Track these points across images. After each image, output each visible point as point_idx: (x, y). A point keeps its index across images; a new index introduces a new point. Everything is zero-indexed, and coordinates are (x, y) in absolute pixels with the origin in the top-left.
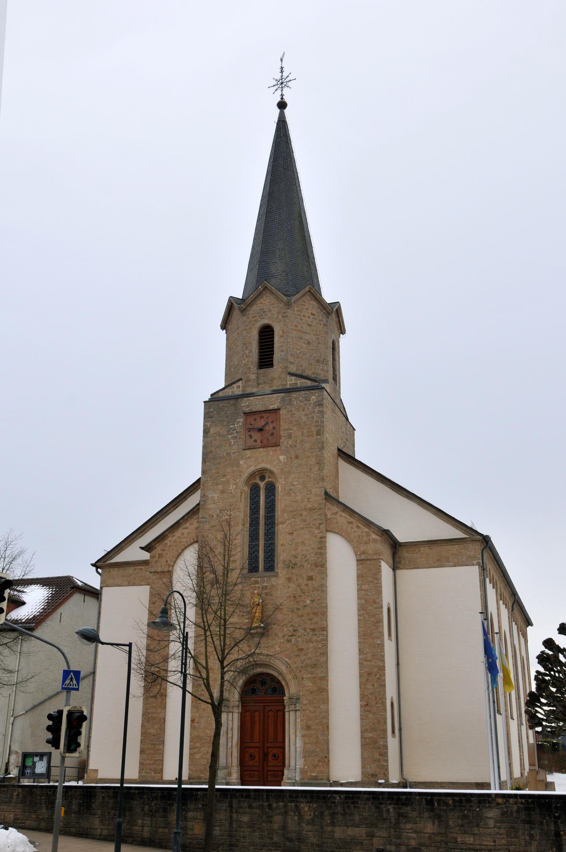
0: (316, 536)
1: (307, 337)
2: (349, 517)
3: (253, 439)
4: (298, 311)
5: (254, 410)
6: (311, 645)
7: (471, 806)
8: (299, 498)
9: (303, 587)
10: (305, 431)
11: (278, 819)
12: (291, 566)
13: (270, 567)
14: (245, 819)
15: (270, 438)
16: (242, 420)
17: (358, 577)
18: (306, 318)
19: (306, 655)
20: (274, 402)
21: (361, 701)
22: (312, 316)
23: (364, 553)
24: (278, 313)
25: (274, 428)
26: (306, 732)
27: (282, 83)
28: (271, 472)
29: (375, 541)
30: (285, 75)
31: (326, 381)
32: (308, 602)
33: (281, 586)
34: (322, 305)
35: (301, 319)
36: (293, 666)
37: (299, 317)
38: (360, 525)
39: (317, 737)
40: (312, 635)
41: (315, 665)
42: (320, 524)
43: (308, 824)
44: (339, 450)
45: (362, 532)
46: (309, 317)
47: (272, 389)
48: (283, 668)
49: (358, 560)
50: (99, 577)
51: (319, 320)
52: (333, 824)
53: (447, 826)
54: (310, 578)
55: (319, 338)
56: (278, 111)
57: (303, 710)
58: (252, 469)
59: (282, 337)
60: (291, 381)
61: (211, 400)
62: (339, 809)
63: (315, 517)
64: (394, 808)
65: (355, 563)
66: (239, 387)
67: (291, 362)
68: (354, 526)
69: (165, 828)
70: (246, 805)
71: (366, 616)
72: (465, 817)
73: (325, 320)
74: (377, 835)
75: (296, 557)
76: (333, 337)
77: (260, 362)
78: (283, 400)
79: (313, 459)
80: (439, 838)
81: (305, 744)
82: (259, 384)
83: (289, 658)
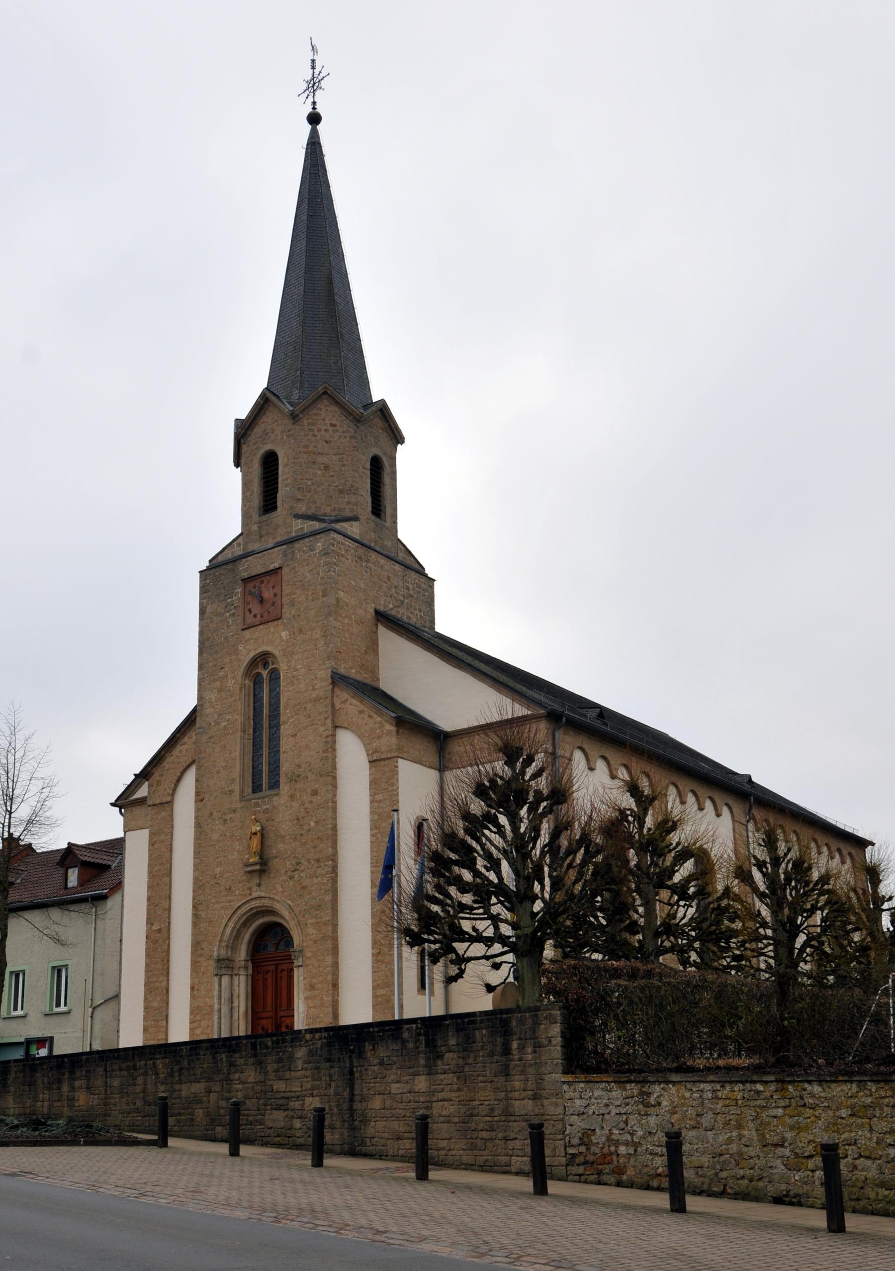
0: (321, 736)
1: (324, 459)
2: (360, 704)
3: (253, 613)
4: (309, 424)
5: (253, 574)
6: (315, 881)
7: (285, 1047)
8: (302, 686)
9: (307, 805)
10: (310, 593)
11: (140, 1080)
12: (295, 779)
13: (275, 785)
14: (116, 1083)
16: (240, 590)
17: (371, 782)
18: (323, 432)
19: (310, 894)
20: (274, 560)
21: (373, 948)
22: (331, 429)
23: (376, 751)
24: (283, 432)
25: (275, 595)
27: (314, 85)
28: (274, 656)
29: (389, 733)
30: (317, 71)
31: (355, 519)
32: (313, 824)
33: (283, 806)
34: (346, 409)
35: (314, 436)
37: (311, 433)
38: (372, 714)
39: (322, 998)
41: (320, 906)
42: (326, 719)
43: (162, 1083)
44: (377, 612)
45: (375, 723)
46: (326, 430)
47: (275, 541)
48: (285, 913)
49: (370, 762)
50: (122, 818)
51: (344, 432)
52: (180, 1082)
53: (266, 1072)
54: (315, 793)
55: (342, 458)
56: (308, 127)
58: (252, 654)
59: (286, 465)
60: (299, 526)
61: (208, 569)
62: (185, 1063)
63: (321, 710)
64: (227, 1056)
65: (367, 765)
66: (239, 545)
67: (299, 500)
68: (366, 716)
69: (59, 1101)
71: (379, 836)
72: (280, 1060)
73: (352, 430)
74: (213, 1089)
75: (299, 766)
76: (375, 451)
77: (265, 506)
78: (285, 554)
79: (319, 631)
80: (258, 1088)
81: (309, 1008)
82: (261, 537)
83: (291, 900)
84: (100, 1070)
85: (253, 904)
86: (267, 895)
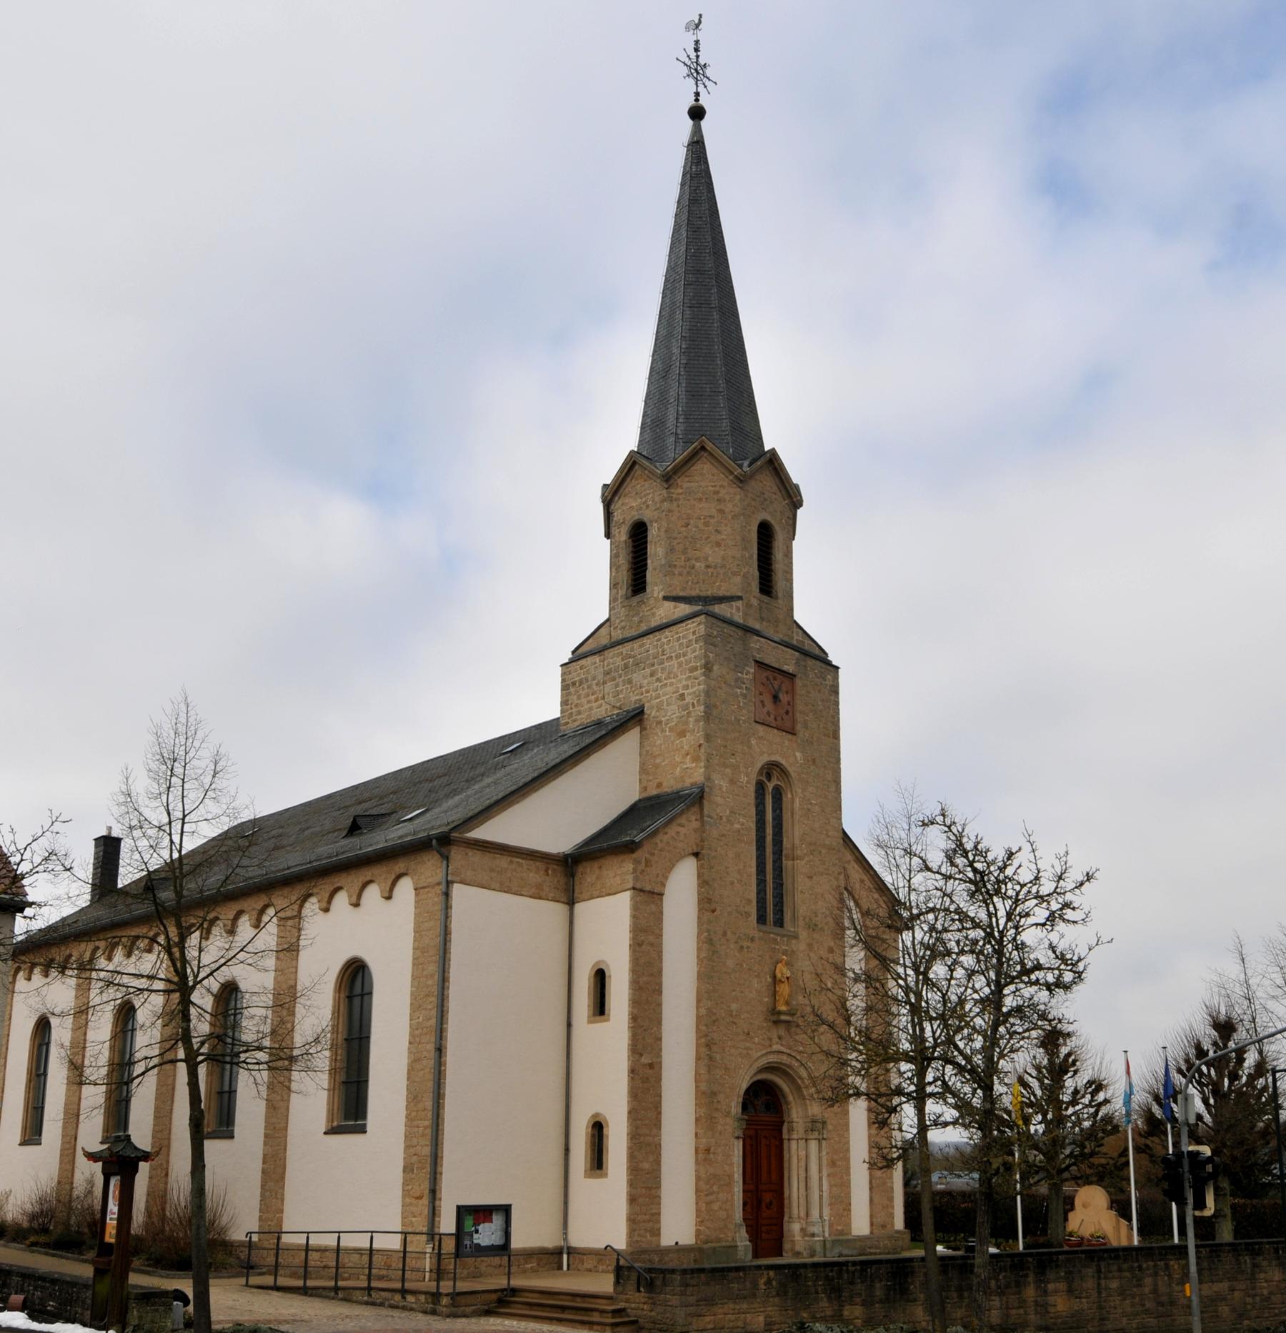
11: (1148, 1281)
14: (1114, 1284)
15: (785, 717)
28: (784, 772)
70: (1115, 1268)
84: (1090, 1271)
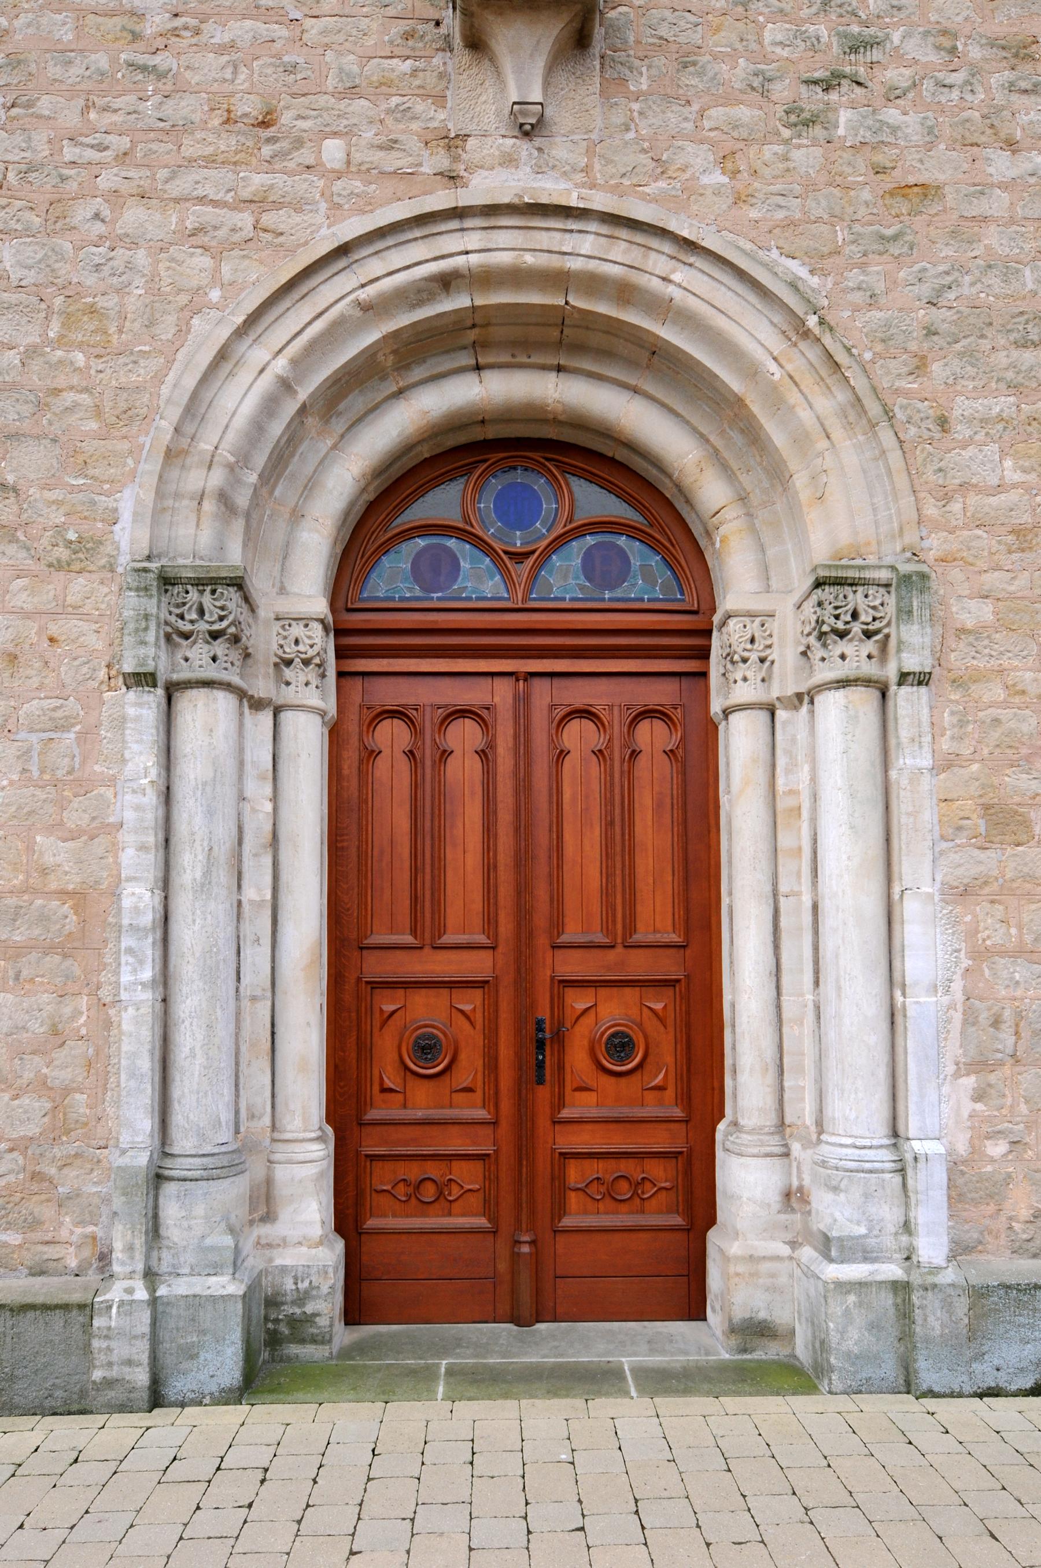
6: (1001, 165)
26: (989, 861)
36: (857, 325)
40: (1011, 87)
57: (956, 682)
81: (981, 954)
83: (819, 260)
85: (467, 248)
86: (600, 201)
